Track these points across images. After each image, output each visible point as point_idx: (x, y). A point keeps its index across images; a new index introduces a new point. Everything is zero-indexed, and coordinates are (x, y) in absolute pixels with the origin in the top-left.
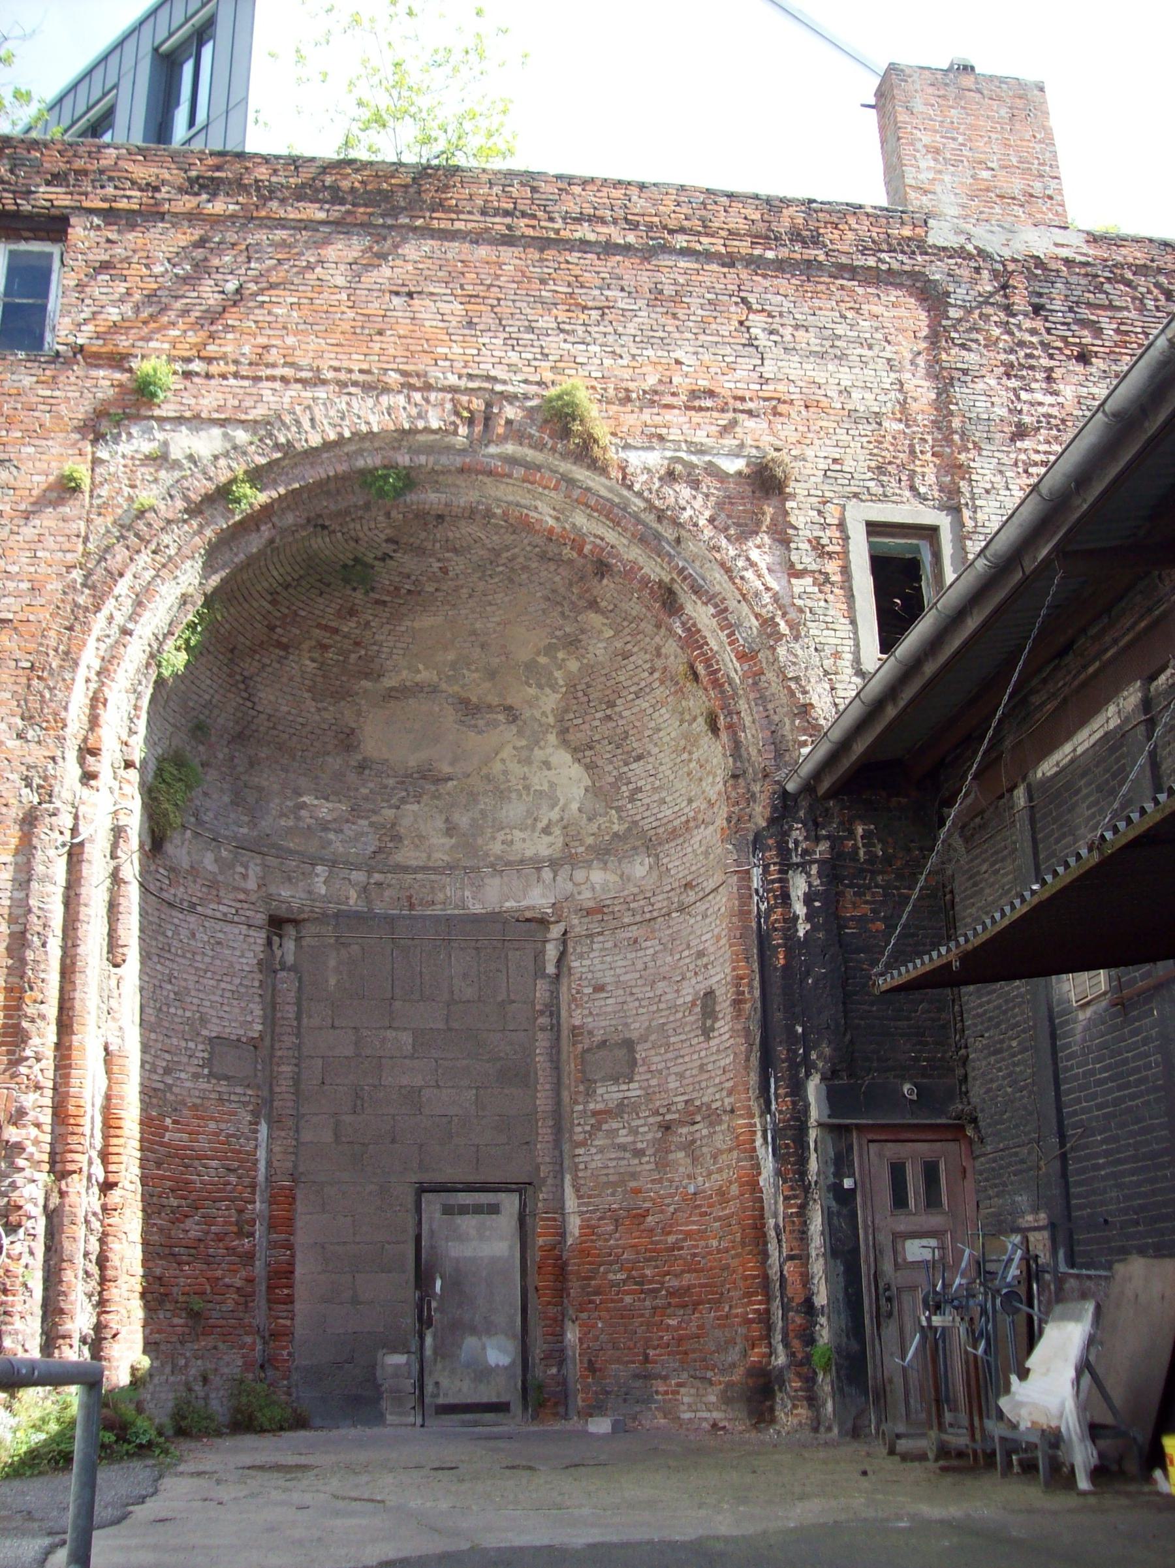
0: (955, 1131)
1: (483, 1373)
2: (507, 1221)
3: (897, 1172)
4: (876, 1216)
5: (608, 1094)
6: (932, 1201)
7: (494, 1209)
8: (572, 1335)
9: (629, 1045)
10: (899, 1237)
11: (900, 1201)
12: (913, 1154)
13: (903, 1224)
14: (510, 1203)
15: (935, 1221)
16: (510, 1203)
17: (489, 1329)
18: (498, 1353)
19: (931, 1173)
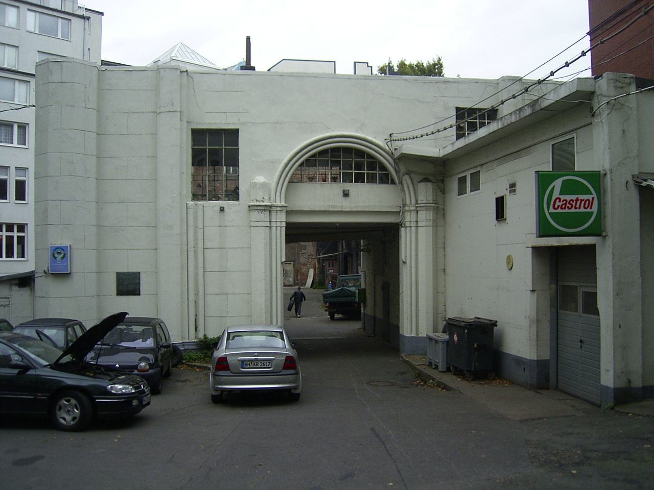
0: (335, 260)
1: (289, 281)
2: (292, 265)
3: (329, 263)
4: (327, 267)
5: (303, 251)
6: (333, 266)
7: (291, 264)
8: (299, 277)
9: (306, 246)
10: (329, 270)
11: (329, 266)
12: (331, 261)
13: (329, 268)
14: (293, 263)
15: (333, 268)
16: (293, 263)
17: (290, 276)
18: (291, 279)
19: (333, 263)
